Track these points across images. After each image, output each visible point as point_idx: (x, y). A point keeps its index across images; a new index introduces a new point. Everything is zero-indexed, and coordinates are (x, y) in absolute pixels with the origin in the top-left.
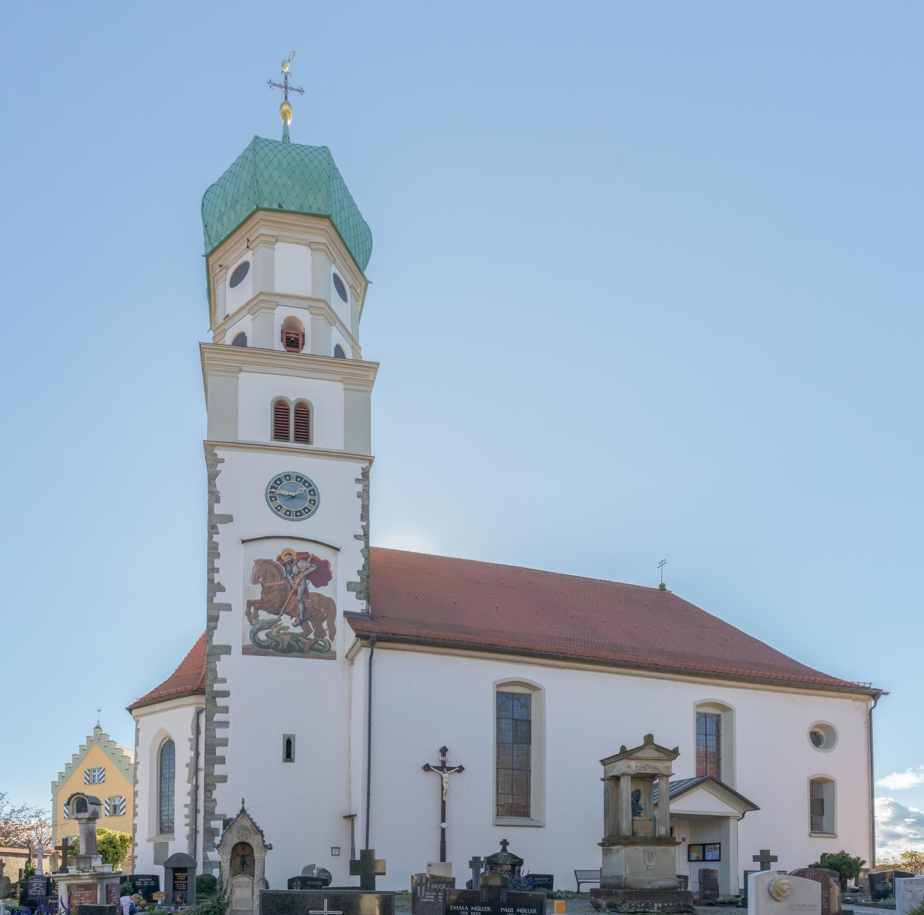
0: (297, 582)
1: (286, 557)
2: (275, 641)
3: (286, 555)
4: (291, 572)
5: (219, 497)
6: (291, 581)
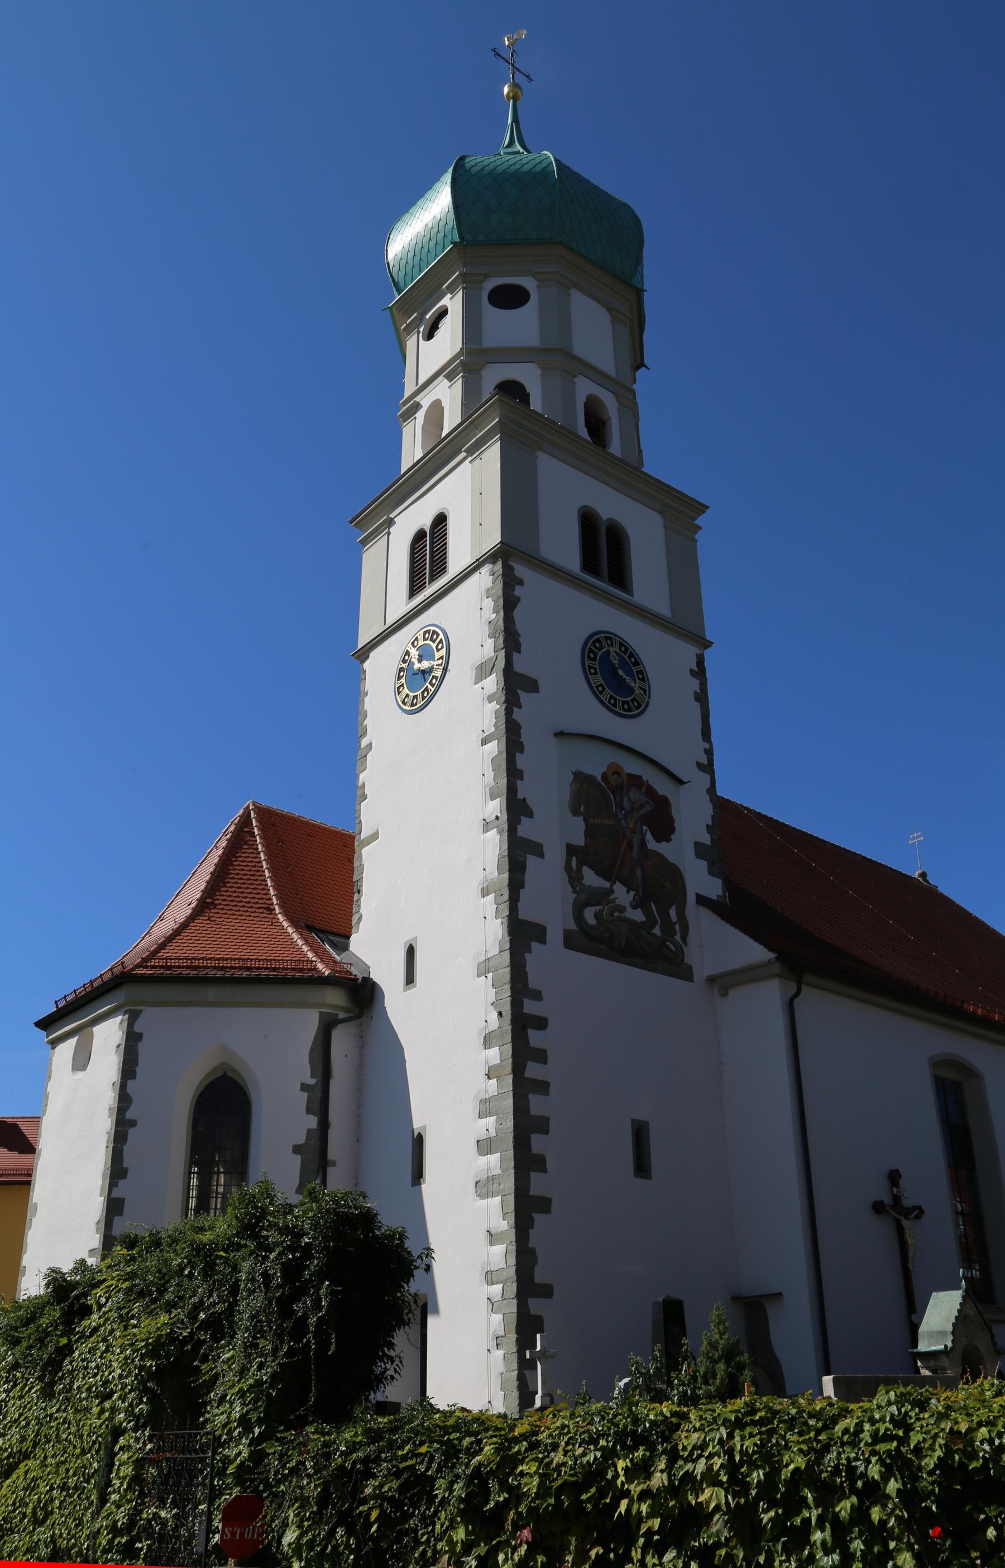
0: (631, 826)
4: (622, 808)
5: (520, 643)
6: (623, 822)
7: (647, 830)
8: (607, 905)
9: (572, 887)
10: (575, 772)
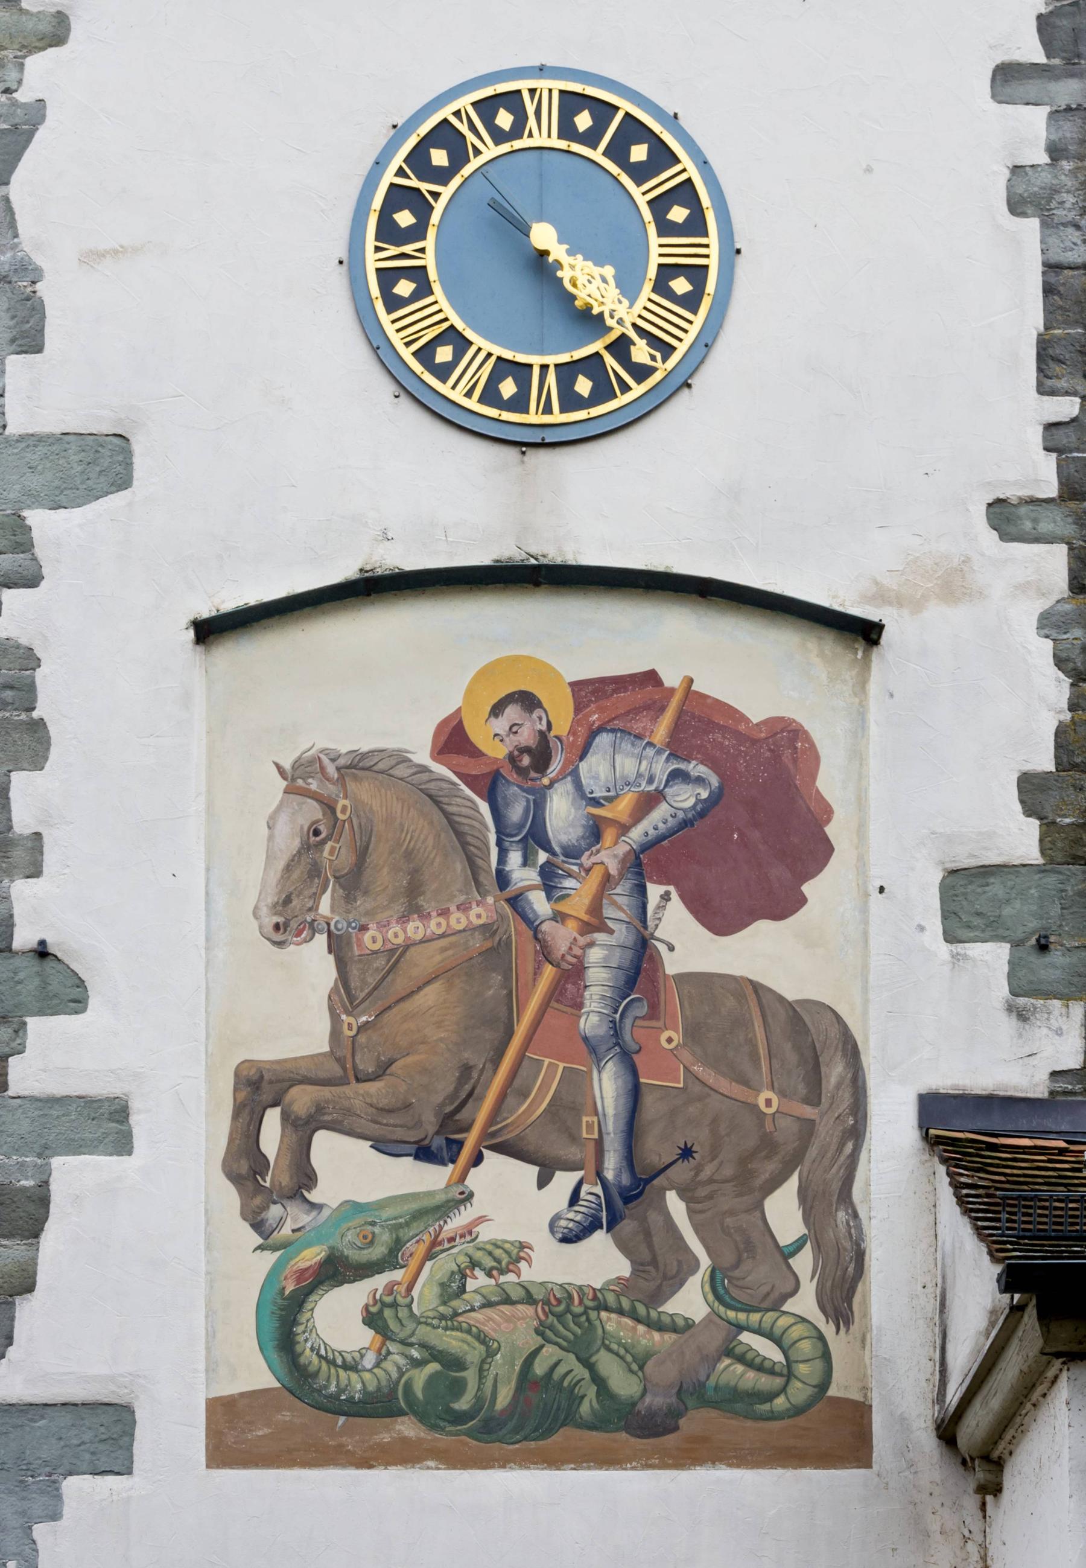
0: (578, 904)
1: (500, 725)
2: (434, 1354)
3: (497, 710)
6: (539, 903)
7: (666, 897)
8: (429, 1256)
9: (258, 1226)
10: (297, 764)
